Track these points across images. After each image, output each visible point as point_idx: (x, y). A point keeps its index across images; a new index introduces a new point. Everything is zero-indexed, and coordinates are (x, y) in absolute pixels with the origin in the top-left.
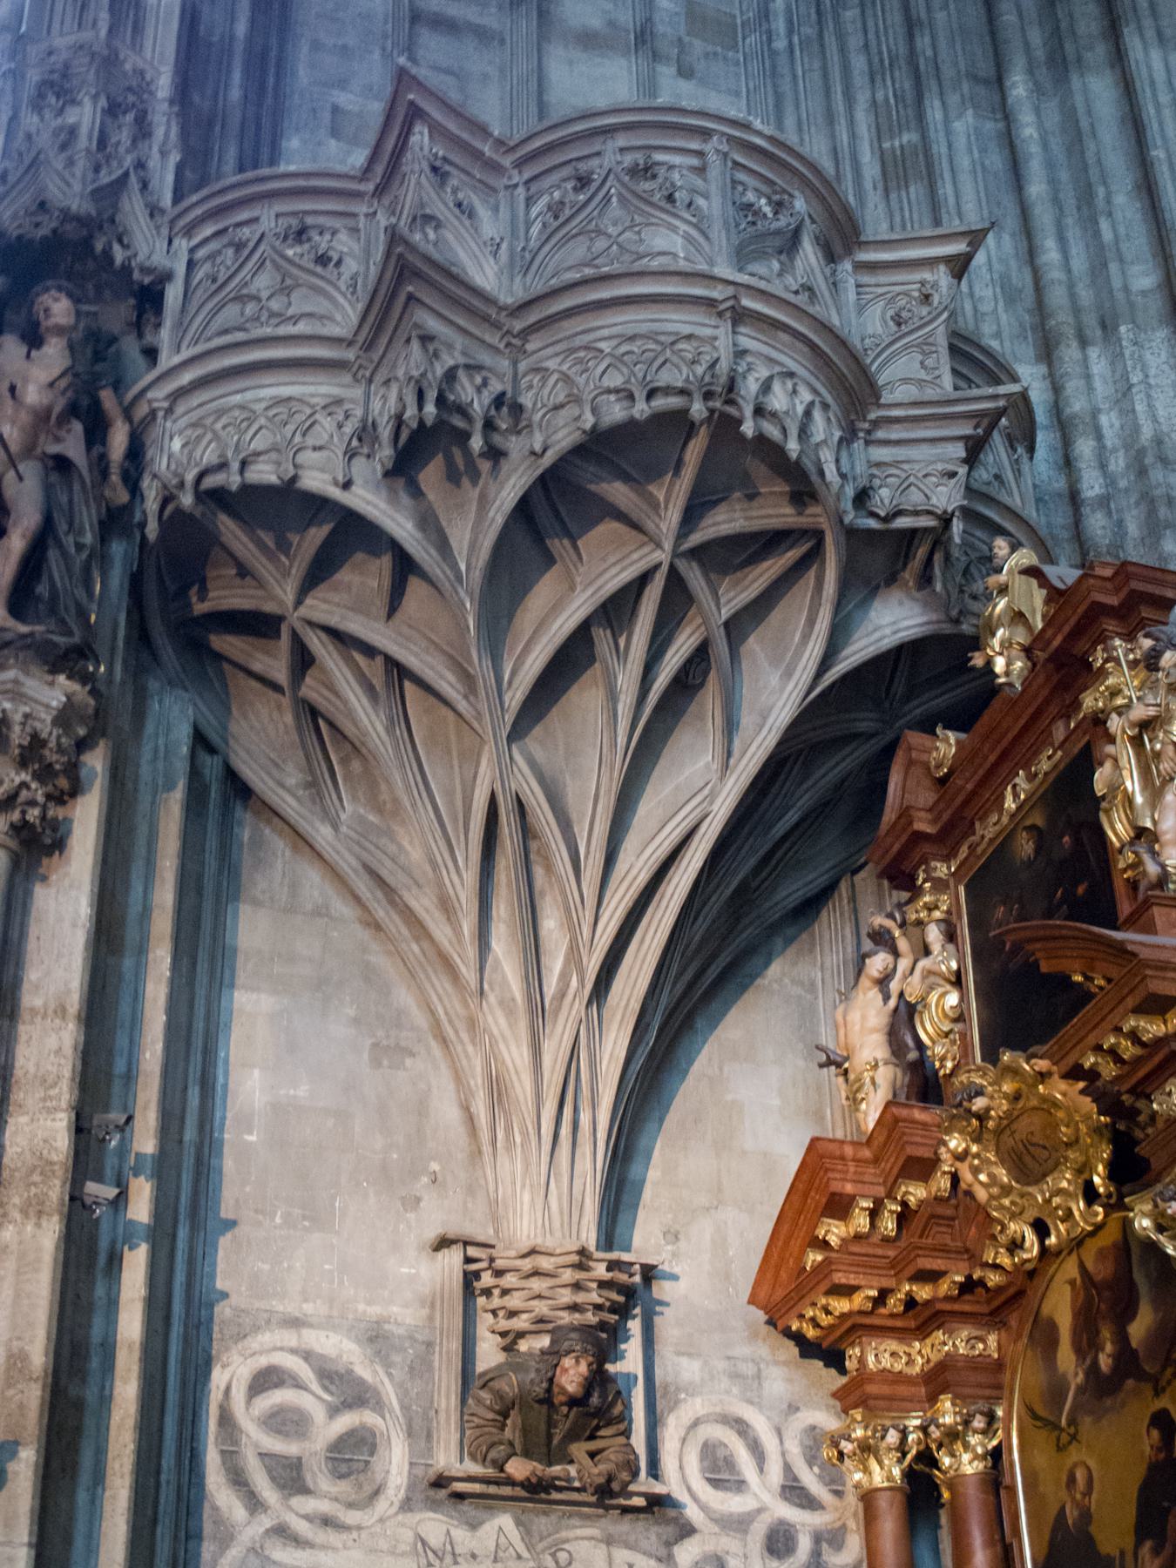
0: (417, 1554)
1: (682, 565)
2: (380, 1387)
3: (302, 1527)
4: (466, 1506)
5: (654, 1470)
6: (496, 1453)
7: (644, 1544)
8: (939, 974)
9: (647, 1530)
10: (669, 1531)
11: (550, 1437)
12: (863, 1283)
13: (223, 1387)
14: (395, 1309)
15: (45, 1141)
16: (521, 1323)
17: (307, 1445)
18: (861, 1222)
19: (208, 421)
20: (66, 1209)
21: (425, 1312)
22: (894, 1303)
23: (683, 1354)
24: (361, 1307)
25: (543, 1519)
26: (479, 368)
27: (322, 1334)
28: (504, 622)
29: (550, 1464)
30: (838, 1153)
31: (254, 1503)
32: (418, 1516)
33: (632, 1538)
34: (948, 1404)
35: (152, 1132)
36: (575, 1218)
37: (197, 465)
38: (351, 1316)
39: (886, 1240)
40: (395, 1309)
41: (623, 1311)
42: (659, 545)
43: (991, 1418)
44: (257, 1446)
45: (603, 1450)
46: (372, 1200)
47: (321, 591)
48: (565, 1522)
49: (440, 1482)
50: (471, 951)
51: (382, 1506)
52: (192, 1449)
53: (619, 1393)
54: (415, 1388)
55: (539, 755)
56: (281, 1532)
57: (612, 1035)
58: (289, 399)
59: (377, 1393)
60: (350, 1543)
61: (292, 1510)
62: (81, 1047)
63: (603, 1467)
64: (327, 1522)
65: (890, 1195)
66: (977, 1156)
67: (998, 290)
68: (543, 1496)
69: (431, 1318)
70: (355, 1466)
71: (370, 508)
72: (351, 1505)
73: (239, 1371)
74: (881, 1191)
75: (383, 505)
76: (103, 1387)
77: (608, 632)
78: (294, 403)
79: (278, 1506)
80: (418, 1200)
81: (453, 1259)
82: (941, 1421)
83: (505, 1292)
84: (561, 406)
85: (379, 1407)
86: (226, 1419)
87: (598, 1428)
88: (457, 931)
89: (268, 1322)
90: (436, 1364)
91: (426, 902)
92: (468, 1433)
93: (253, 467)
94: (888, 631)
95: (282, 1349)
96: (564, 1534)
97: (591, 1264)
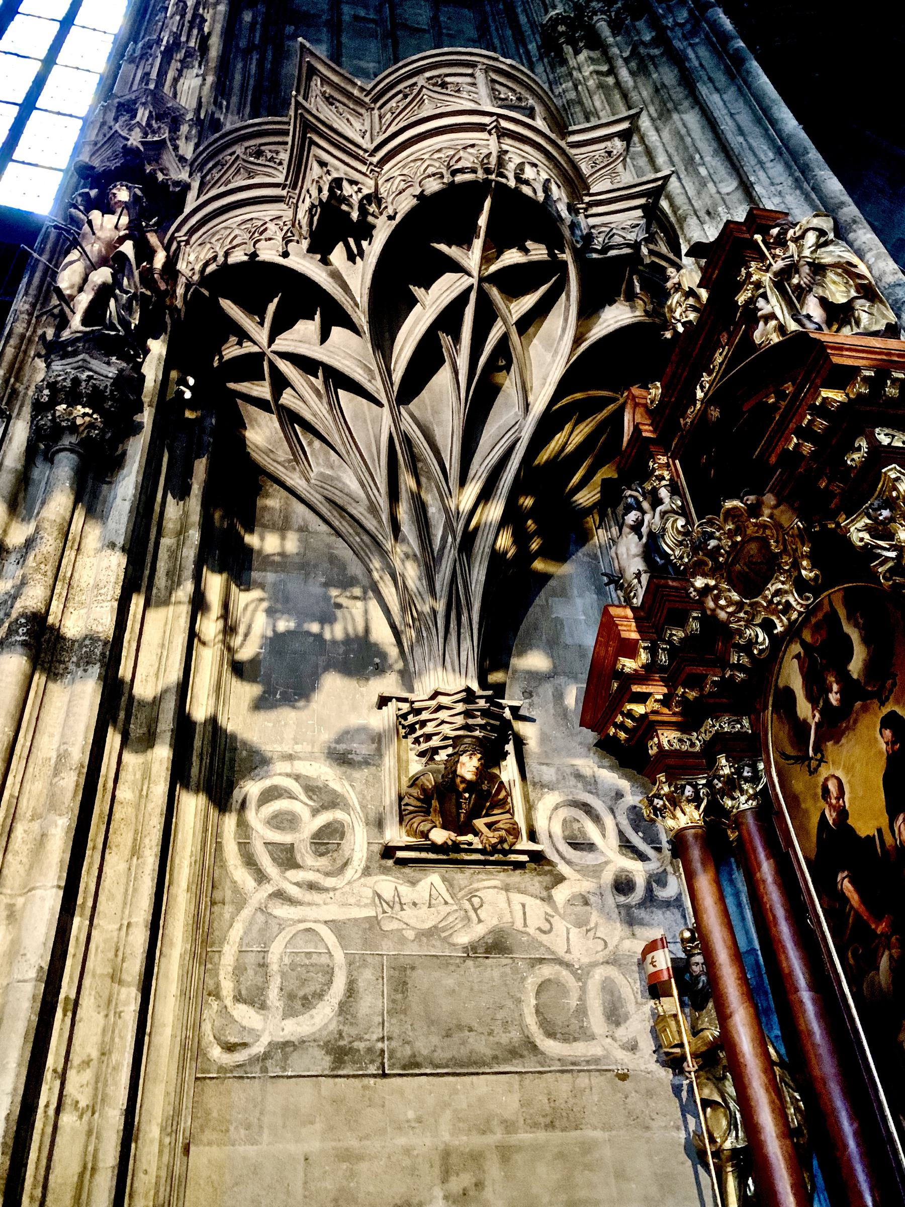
0: (376, 906)
2: (346, 795)
3: (294, 891)
4: (407, 870)
10: (547, 879)
13: (240, 801)
16: (435, 742)
17: (297, 835)
23: (543, 764)
31: (261, 877)
33: (522, 886)
48: (476, 877)
49: (388, 852)
51: (350, 873)
54: (369, 793)
56: (280, 895)
64: (312, 886)
72: (327, 874)
85: (346, 806)
88: (380, 521)
97: (477, 700)
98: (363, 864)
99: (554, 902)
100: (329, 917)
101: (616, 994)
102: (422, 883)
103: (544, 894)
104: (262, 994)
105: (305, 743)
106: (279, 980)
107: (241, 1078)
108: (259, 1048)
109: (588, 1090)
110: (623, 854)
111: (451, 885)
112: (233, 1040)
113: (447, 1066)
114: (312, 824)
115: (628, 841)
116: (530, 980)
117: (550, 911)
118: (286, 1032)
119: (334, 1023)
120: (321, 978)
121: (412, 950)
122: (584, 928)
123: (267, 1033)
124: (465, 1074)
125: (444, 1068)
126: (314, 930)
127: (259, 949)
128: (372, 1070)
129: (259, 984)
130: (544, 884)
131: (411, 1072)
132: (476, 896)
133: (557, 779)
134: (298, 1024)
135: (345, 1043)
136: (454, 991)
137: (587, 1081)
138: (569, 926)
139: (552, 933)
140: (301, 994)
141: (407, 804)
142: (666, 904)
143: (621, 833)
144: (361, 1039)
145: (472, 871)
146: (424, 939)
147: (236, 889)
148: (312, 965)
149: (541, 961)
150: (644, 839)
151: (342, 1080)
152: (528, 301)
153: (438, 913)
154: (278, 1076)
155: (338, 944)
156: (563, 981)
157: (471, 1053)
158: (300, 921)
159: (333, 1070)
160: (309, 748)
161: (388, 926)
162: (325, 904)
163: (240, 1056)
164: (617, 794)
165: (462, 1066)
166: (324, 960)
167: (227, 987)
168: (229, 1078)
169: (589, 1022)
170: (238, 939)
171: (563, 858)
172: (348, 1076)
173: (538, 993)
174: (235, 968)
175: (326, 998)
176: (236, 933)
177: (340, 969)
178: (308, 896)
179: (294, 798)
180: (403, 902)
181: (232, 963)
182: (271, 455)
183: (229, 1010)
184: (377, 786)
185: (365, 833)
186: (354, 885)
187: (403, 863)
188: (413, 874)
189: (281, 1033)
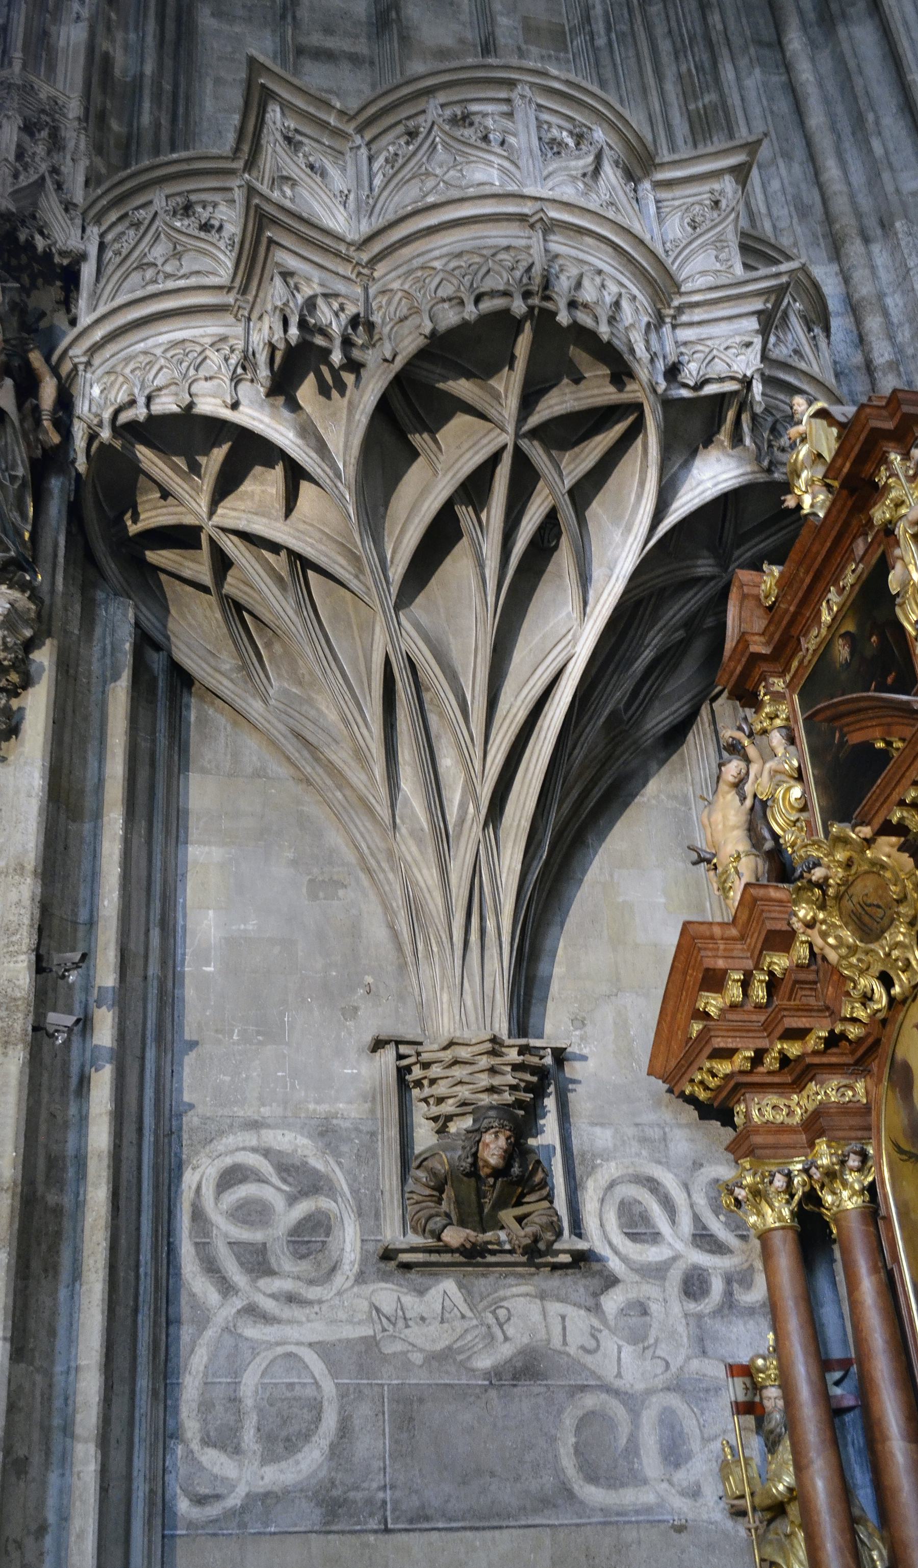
0: (373, 1322)
1: (524, 444)
2: (332, 1175)
3: (268, 1305)
4: (413, 1275)
5: (577, 1228)
6: (439, 1221)
7: (574, 1297)
8: (783, 772)
9: (575, 1283)
10: (595, 1283)
11: (481, 1207)
12: (739, 1046)
13: (194, 1187)
14: (341, 1105)
15: (9, 981)
17: (270, 1231)
18: (735, 992)
19: (119, 369)
20: (29, 1039)
21: (368, 1106)
22: (771, 1062)
24: (311, 1106)
25: (482, 1281)
26: (336, 295)
27: (279, 1132)
28: (382, 509)
29: (484, 1231)
30: (708, 933)
31: (226, 1288)
32: (372, 1287)
34: (824, 1147)
35: (112, 967)
36: (488, 1013)
37: (112, 404)
38: (303, 1115)
39: (759, 1007)
40: (341, 1105)
41: (539, 1091)
42: (507, 432)
43: (864, 1156)
44: (226, 1236)
46: (316, 1013)
47: (229, 501)
48: (502, 1282)
49: (388, 1255)
50: (383, 791)
51: (339, 1280)
52: (169, 1244)
53: (538, 1162)
55: (424, 620)
56: (251, 1311)
57: (509, 852)
58: (184, 341)
59: (329, 1180)
60: (313, 1316)
61: (261, 1291)
62: (38, 898)
63: (529, 1230)
64: (291, 1299)
65: (758, 967)
66: (823, 922)
67: (792, 209)
68: (479, 1259)
69: (372, 1111)
70: (313, 1246)
71: (256, 423)
72: (311, 1282)
73: (208, 1171)
74: (749, 964)
75: (267, 420)
76: (78, 1194)
77: (470, 509)
78: (187, 344)
79: (248, 1288)
80: (356, 1009)
81: (388, 1056)
82: (819, 1162)
83: (433, 1082)
84: (406, 318)
86: (198, 1215)
87: (523, 1195)
89: (231, 1126)
90: (380, 1150)
91: (344, 755)
92: (409, 1208)
93: (157, 400)
94: (709, 484)
95: (244, 1149)
96: (501, 1293)
97: (504, 1050)
99: (603, 1312)
100: (314, 1338)
101: (678, 1428)
102: (433, 1291)
103: (590, 1302)
104: (235, 1436)
105: (274, 1104)
106: (255, 1418)
107: (215, 1535)
108: (234, 1501)
109: (634, 1546)
110: (698, 1246)
111: (470, 1293)
112: (203, 1490)
113: (464, 1519)
115: (705, 1228)
117: (596, 1323)
118: (266, 1480)
119: (325, 1468)
120: (307, 1416)
121: (419, 1378)
122: (641, 1346)
123: (243, 1481)
124: (484, 1528)
125: (458, 1520)
126: (296, 1355)
127: (229, 1380)
128: (373, 1524)
129: (232, 1423)
130: (591, 1289)
131: (419, 1526)
132: (501, 1307)
133: (615, 1145)
134: (281, 1471)
135: (339, 1493)
136: (473, 1428)
137: (634, 1534)
138: (621, 1343)
139: (600, 1353)
140: (284, 1434)
141: (412, 1192)
142: (751, 1311)
143: (696, 1218)
144: (357, 1488)
146: (435, 1364)
147: (197, 1305)
148: (295, 1399)
149: (583, 1388)
150: (727, 1225)
151: (336, 1536)
153: (453, 1330)
154: (259, 1533)
155: (326, 1372)
156: (611, 1414)
157: (493, 1503)
158: (278, 1344)
159: (327, 1523)
160: (279, 1111)
161: (390, 1348)
162: (309, 1321)
163: (213, 1510)
164: (694, 1163)
165: (481, 1519)
166: (310, 1392)
168: (201, 1535)
169: (641, 1464)
170: (202, 1368)
171: (616, 1252)
172: (343, 1532)
173: (578, 1430)
174: (200, 1405)
175: (315, 1439)
177: (330, 1403)
178: (286, 1312)
179: (263, 1182)
180: (408, 1316)
181: (196, 1397)
182: (212, 661)
183: (197, 1455)
184: (371, 1162)
185: (358, 1228)
186: (345, 1296)
187: (407, 1267)
188: (420, 1280)
189: (261, 1483)
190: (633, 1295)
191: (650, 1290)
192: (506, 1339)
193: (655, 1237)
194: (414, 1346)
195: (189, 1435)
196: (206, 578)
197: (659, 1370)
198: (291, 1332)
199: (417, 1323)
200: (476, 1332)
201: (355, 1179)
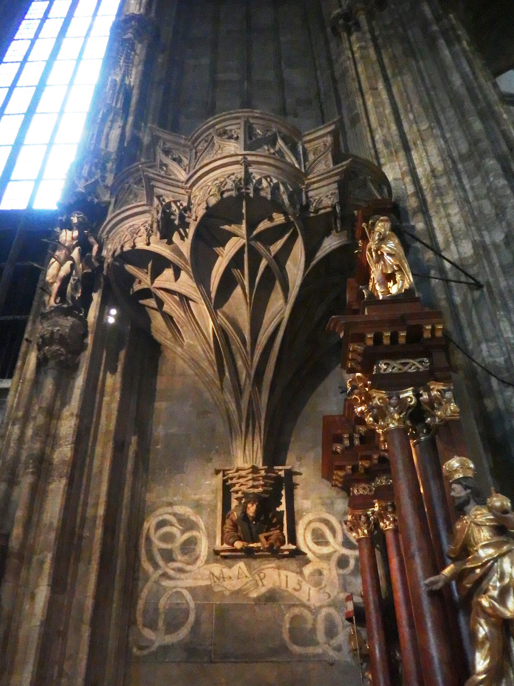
2: (198, 522)
3: (171, 573)
4: (227, 561)
5: (293, 539)
13: (147, 528)
17: (174, 544)
21: (213, 495)
24: (193, 496)
31: (156, 566)
45: (271, 535)
49: (217, 553)
51: (199, 563)
56: (165, 575)
64: (181, 570)
69: (216, 498)
72: (188, 564)
86: (148, 539)
95: (167, 513)
96: (262, 567)
98: (205, 558)
100: (188, 585)
103: (298, 570)
108: (153, 648)
114: (181, 538)
116: (287, 616)
117: (300, 579)
118: (166, 640)
143: (344, 535)
145: (261, 560)
146: (234, 595)
147: (146, 573)
149: (294, 605)
152: (280, 244)
158: (174, 588)
160: (180, 498)
161: (217, 589)
162: (186, 579)
163: (146, 652)
166: (185, 606)
167: (140, 619)
171: (310, 550)
174: (144, 612)
176: (144, 594)
178: (178, 575)
187: (225, 557)
190: (316, 567)
191: (323, 565)
192: (263, 585)
193: (327, 543)
194: (226, 589)
195: (138, 623)
196: (155, 306)
197: (326, 597)
198: (180, 583)
199: (228, 580)
200: (251, 583)
201: (207, 524)
